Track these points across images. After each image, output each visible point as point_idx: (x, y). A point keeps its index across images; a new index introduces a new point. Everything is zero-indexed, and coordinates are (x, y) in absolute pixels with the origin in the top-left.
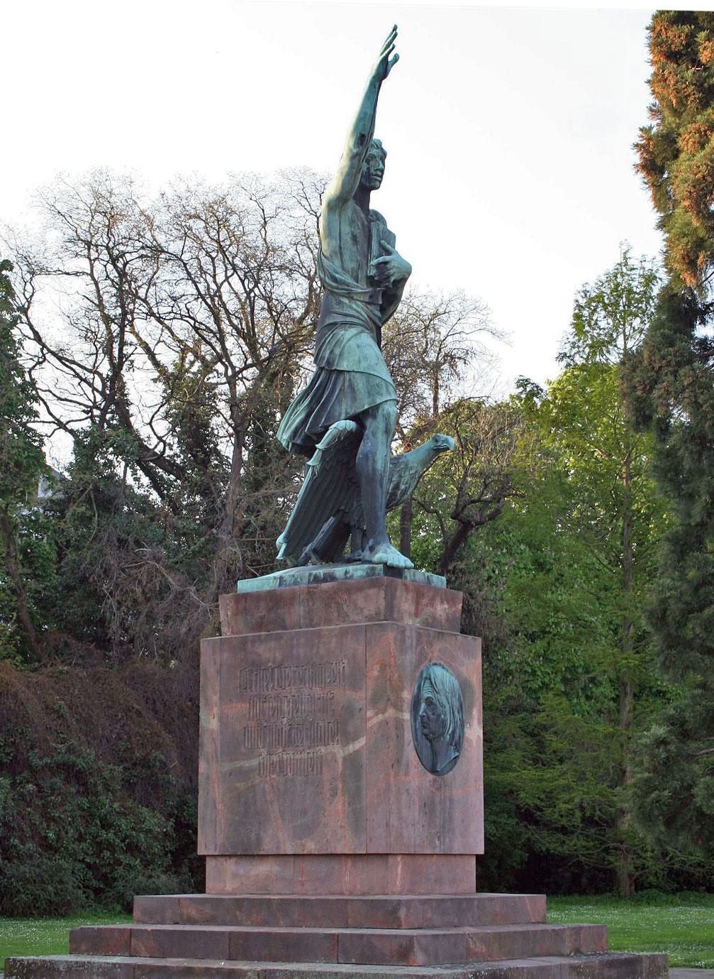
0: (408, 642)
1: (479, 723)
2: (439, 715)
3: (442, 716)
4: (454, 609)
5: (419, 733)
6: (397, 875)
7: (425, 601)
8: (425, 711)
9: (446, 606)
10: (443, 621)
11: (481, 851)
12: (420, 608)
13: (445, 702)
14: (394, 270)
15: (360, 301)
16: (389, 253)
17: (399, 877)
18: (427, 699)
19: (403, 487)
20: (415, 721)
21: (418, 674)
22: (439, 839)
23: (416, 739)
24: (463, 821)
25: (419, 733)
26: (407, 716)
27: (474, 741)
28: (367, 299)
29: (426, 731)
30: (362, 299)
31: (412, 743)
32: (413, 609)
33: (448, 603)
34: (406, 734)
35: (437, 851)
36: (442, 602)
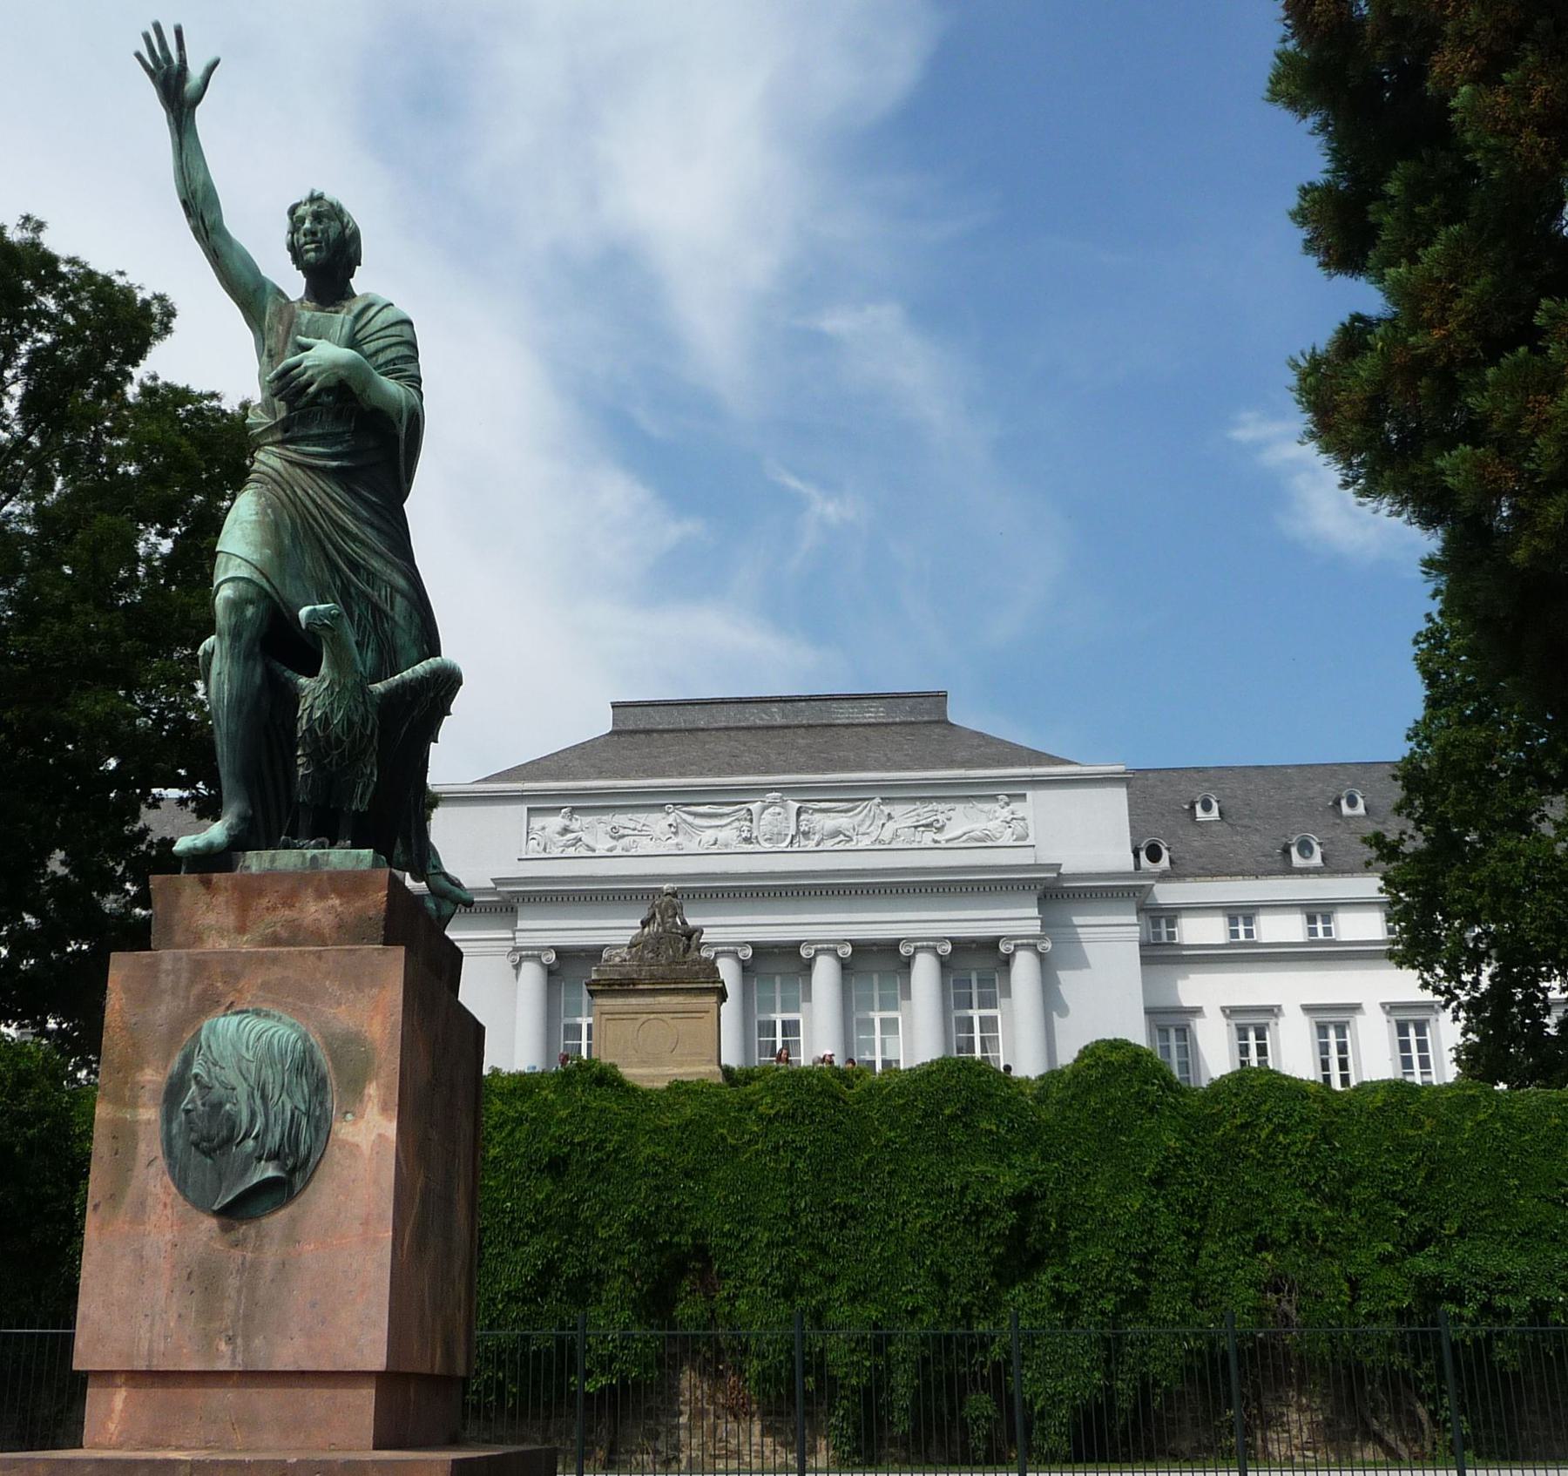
0: (166, 981)
1: (384, 1109)
2: (221, 1105)
3: (228, 1106)
4: (359, 904)
5: (179, 1143)
6: (112, 1411)
7: (264, 902)
8: (192, 1101)
9: (335, 901)
10: (327, 931)
11: (376, 1359)
12: (252, 914)
13: (232, 1076)
14: (309, 373)
15: (269, 444)
16: (307, 348)
17: (116, 1416)
18: (196, 1076)
19: (318, 714)
20: (168, 1118)
21: (188, 1036)
22: (230, 1340)
23: (169, 1151)
24: (313, 1305)
25: (179, 1143)
26: (149, 1113)
27: (366, 1148)
28: (279, 436)
29: (193, 1136)
30: (270, 440)
31: (161, 1163)
32: (230, 920)
33: (340, 895)
34: (142, 1147)
35: (223, 1365)
36: (321, 895)
